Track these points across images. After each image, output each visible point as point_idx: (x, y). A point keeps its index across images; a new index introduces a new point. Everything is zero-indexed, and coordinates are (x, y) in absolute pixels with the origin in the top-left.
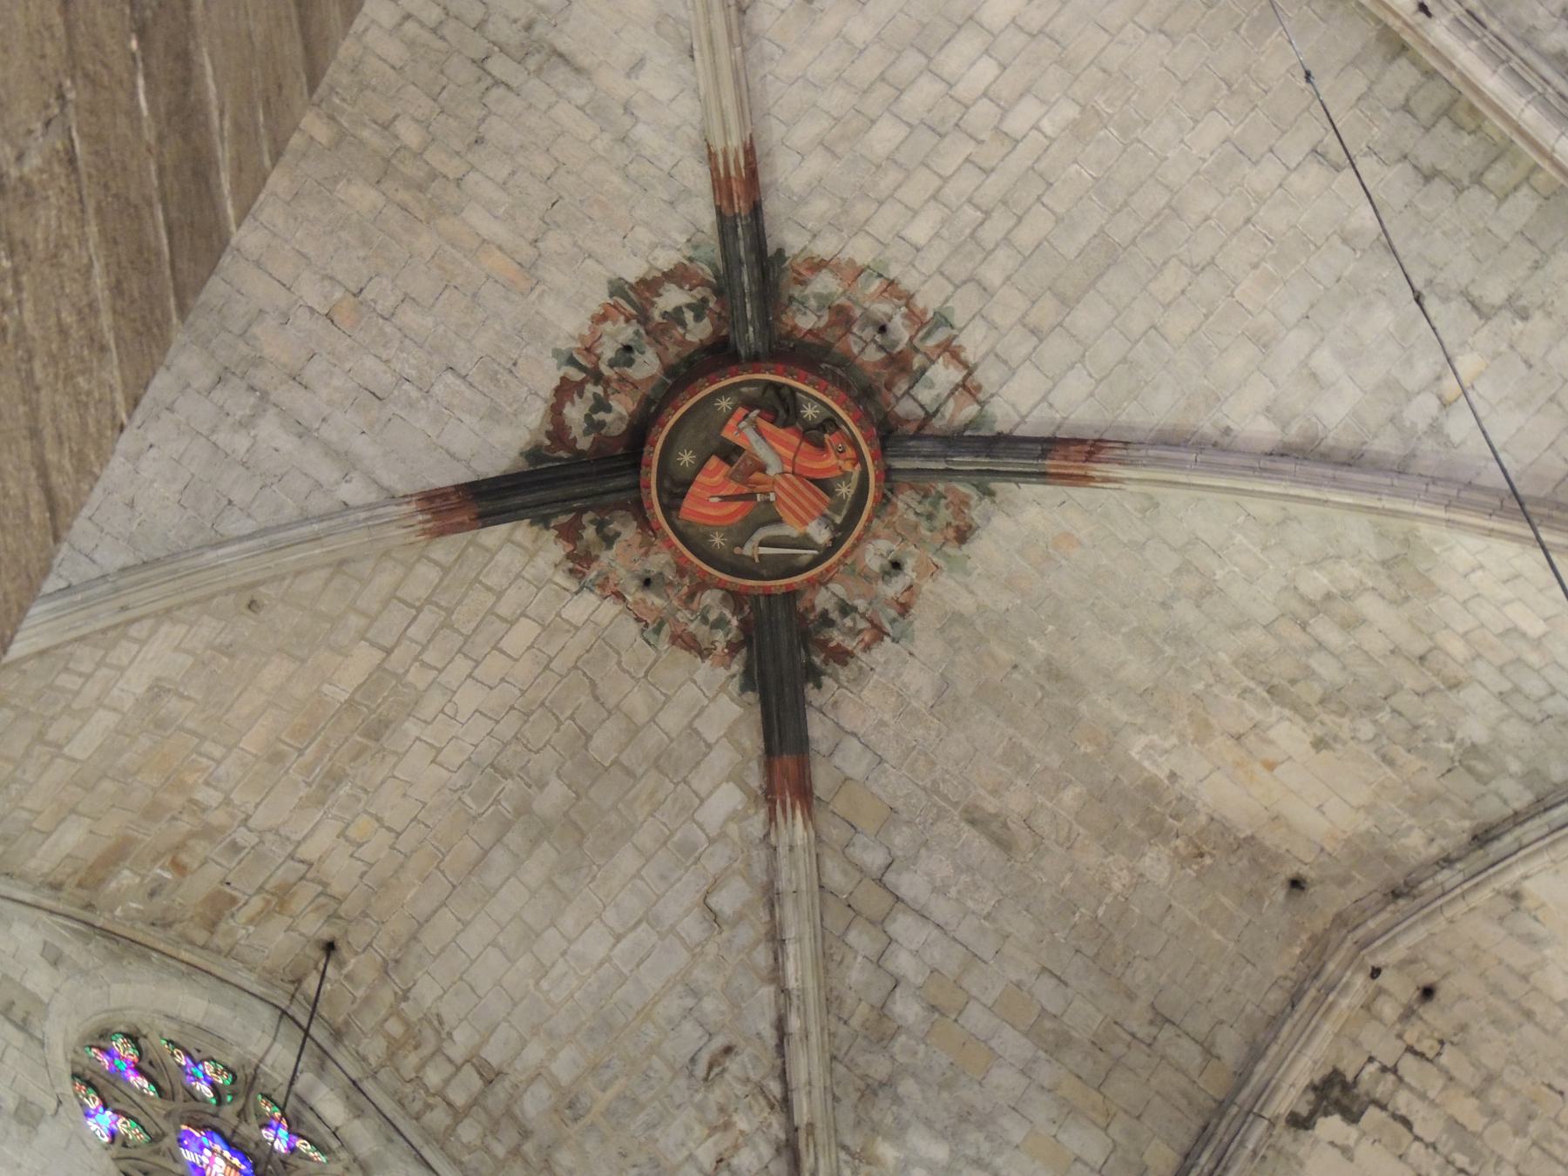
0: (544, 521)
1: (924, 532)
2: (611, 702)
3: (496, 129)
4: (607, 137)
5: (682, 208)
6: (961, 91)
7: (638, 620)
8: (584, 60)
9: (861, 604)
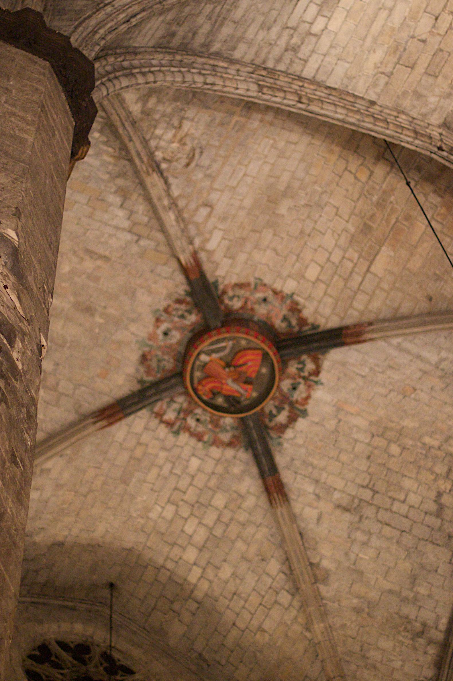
0: (315, 327)
1: (159, 353)
2: (269, 252)
3: (363, 465)
4: (323, 480)
5: (288, 459)
6: (196, 521)
7: (265, 285)
8: (338, 512)
9: (176, 319)
